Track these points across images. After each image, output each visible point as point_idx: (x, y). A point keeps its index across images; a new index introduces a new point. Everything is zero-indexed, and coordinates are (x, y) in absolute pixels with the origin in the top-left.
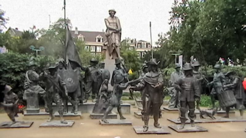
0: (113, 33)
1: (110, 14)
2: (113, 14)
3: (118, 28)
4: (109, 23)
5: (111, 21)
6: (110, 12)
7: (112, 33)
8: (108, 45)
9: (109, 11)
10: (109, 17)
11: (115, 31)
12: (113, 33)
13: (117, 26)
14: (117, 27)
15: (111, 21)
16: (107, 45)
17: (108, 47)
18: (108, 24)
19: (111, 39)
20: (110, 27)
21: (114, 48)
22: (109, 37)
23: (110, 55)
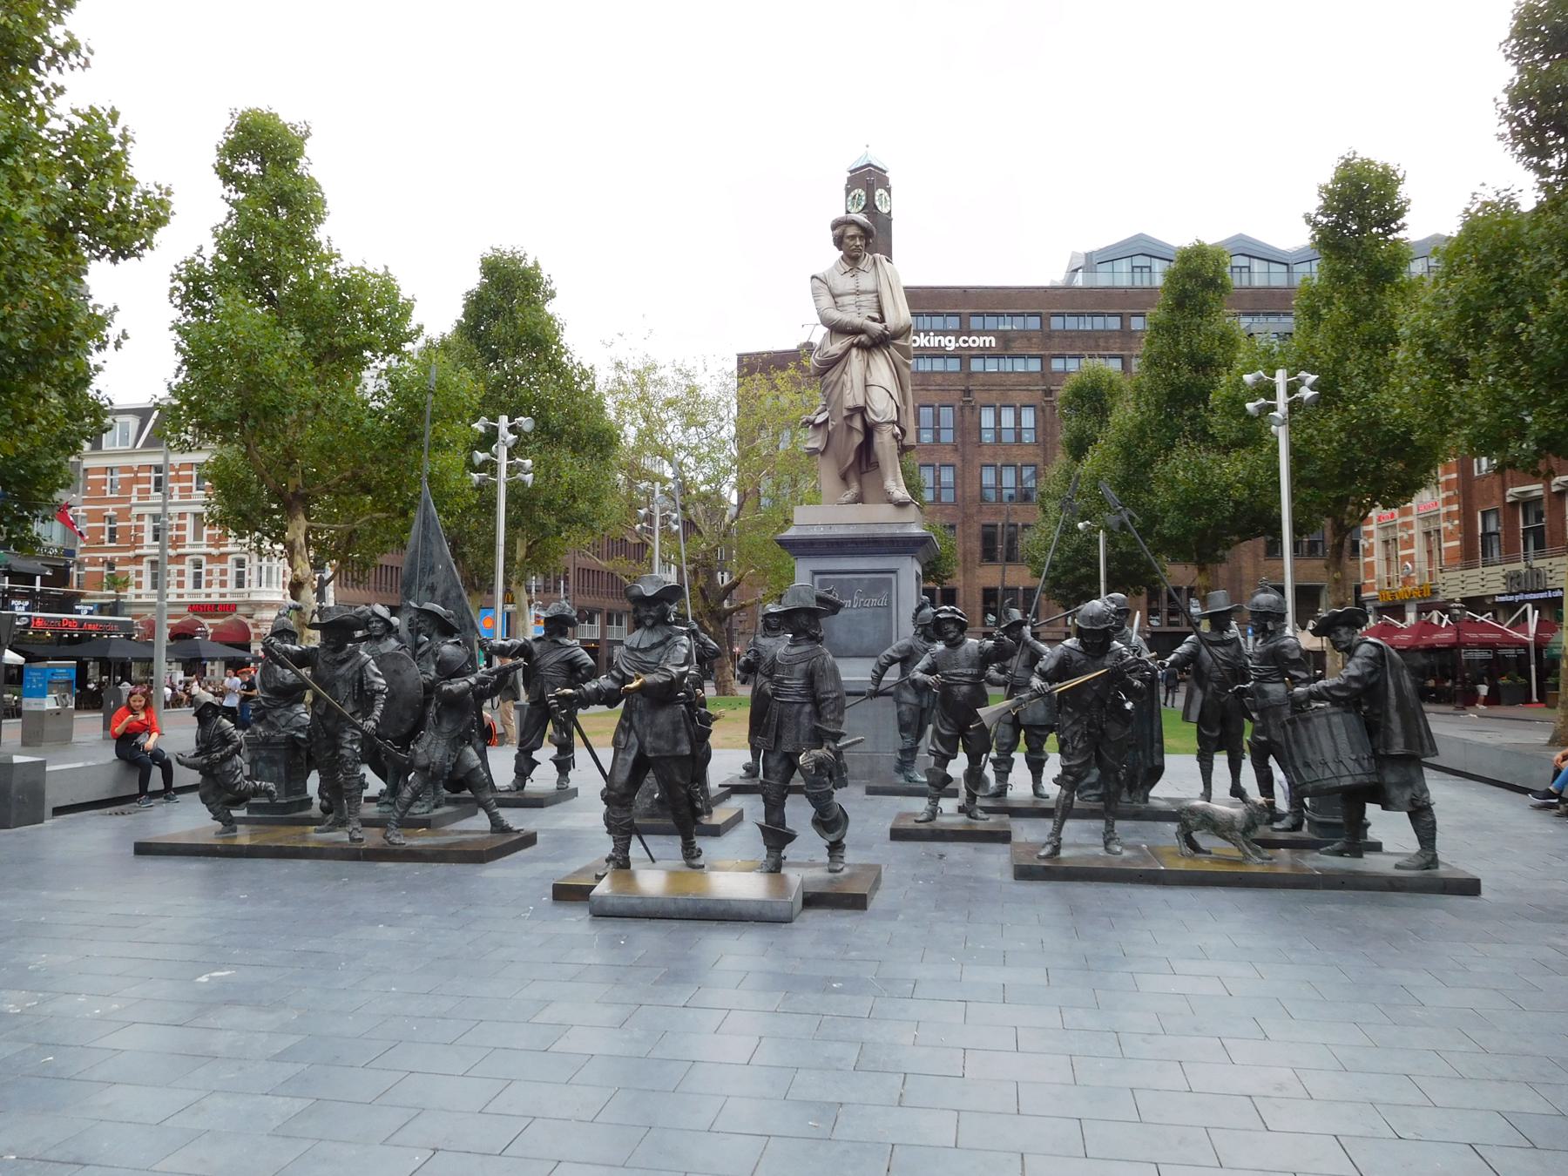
0: (854, 351)
1: (839, 242)
2: (853, 237)
3: (882, 320)
4: (834, 296)
5: (845, 283)
6: (837, 231)
7: (847, 352)
8: (830, 428)
9: (834, 227)
10: (835, 267)
11: (863, 338)
12: (854, 351)
13: (881, 312)
14: (877, 316)
15: (845, 283)
16: (826, 421)
17: (829, 438)
18: (826, 300)
19: (840, 385)
20: (837, 315)
21: (858, 439)
22: (832, 376)
23: (844, 478)
